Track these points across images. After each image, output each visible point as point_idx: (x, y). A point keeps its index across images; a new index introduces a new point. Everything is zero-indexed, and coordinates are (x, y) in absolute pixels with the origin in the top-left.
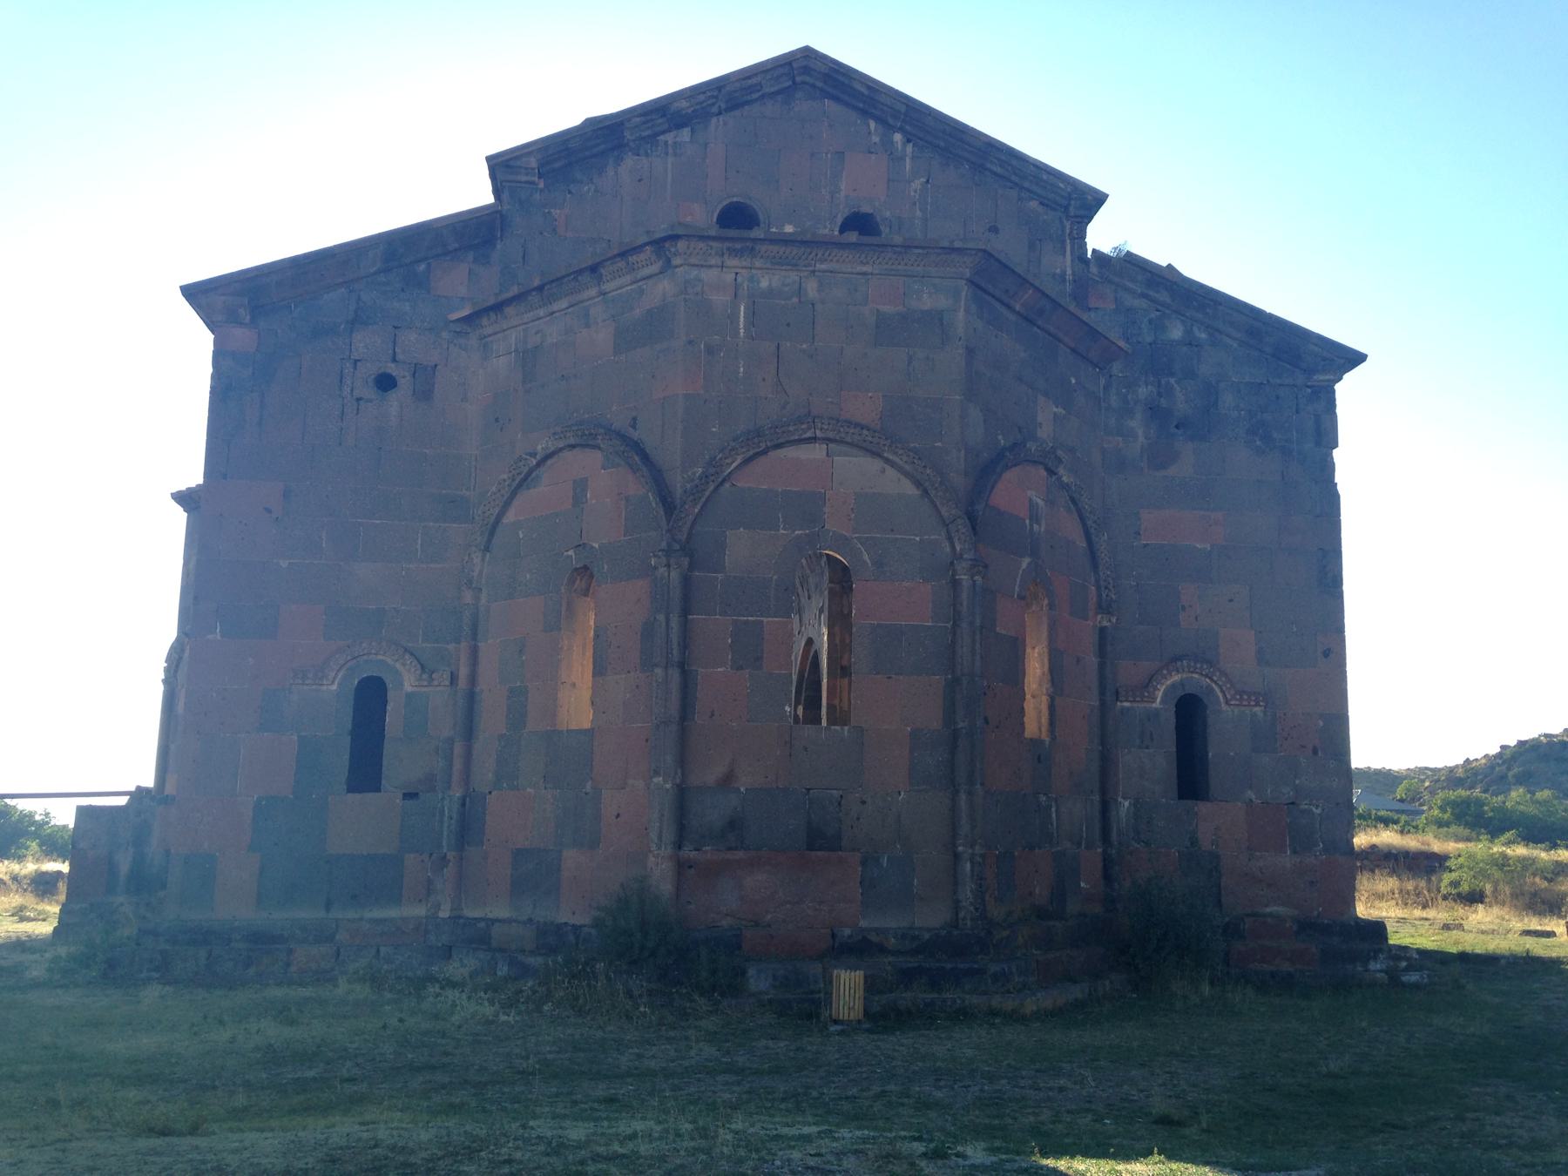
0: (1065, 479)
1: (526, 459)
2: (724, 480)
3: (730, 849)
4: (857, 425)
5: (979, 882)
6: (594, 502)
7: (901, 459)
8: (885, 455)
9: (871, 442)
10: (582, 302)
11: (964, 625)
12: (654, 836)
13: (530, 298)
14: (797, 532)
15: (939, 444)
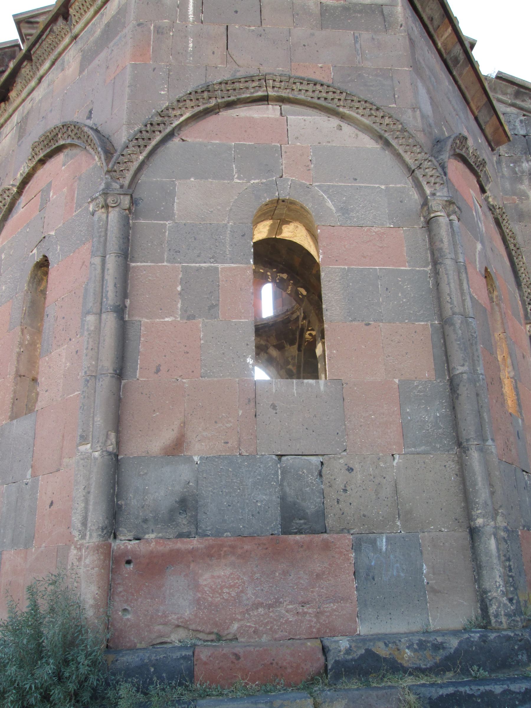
0: (490, 200)
1: (9, 190)
2: (171, 135)
3: (180, 536)
4: (309, 82)
5: (507, 564)
6: (55, 197)
7: (358, 113)
8: (341, 110)
9: (326, 99)
10: (60, 54)
11: (449, 262)
12: (76, 519)
13: (23, 71)
14: (252, 182)
15: (394, 106)
